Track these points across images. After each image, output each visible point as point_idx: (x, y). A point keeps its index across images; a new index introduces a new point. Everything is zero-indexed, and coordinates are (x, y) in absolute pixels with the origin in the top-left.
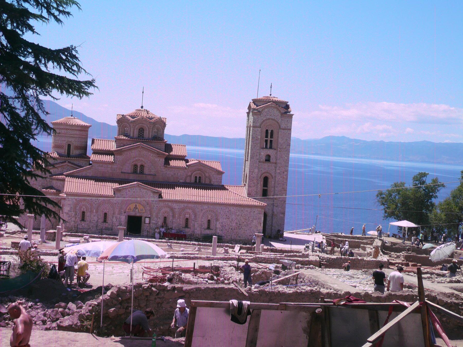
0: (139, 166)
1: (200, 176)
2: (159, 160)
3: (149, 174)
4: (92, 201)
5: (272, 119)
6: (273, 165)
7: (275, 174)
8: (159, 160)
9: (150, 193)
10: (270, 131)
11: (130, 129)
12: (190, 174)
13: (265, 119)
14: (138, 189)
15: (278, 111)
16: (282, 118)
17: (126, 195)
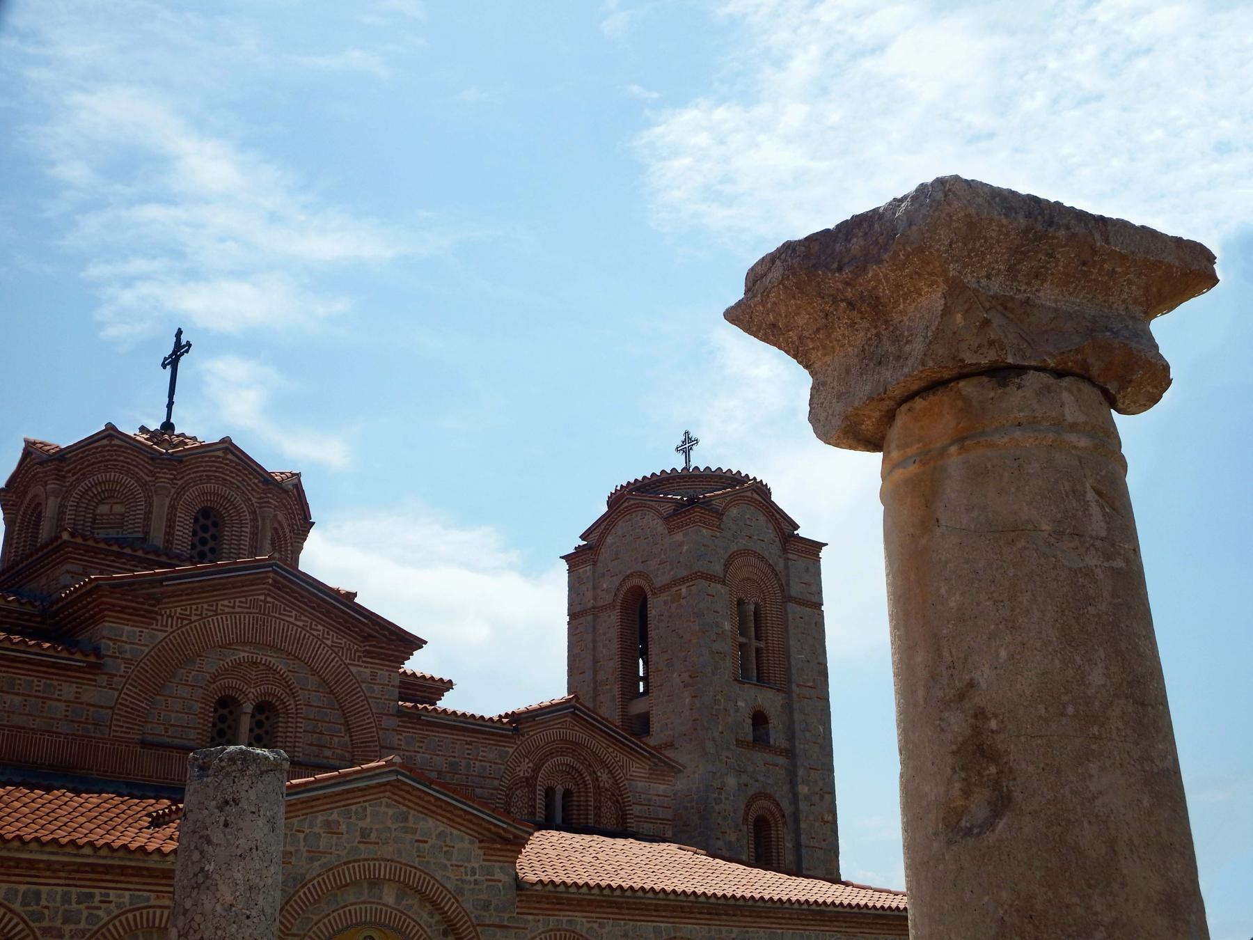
0: (248, 708)
1: (571, 786)
2: (374, 675)
3: (313, 760)
4: (40, 917)
5: (755, 554)
6: (781, 760)
7: (795, 799)
8: (374, 675)
9: (466, 844)
10: (752, 607)
11: (150, 505)
12: (525, 768)
13: (734, 548)
14: (390, 812)
15: (770, 525)
16: (790, 556)
17: (311, 860)
